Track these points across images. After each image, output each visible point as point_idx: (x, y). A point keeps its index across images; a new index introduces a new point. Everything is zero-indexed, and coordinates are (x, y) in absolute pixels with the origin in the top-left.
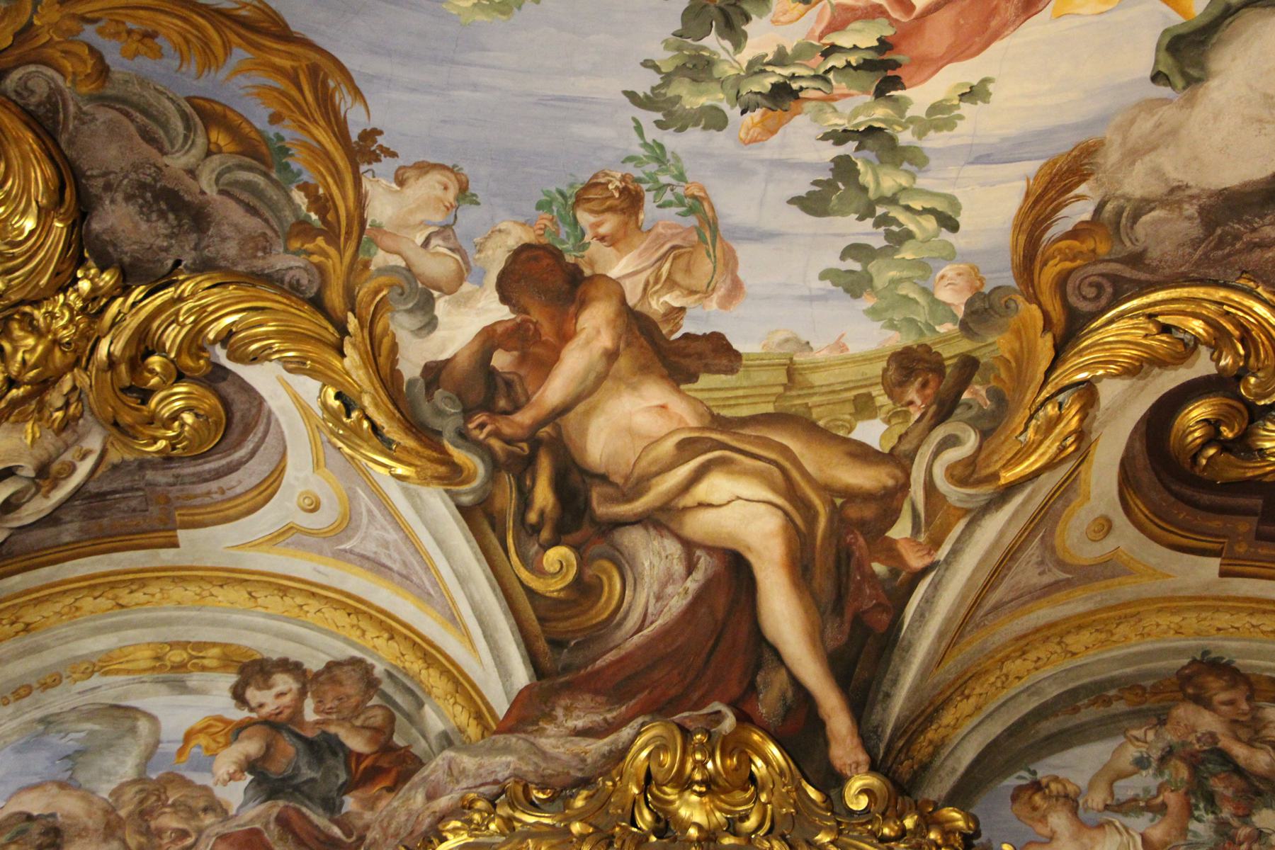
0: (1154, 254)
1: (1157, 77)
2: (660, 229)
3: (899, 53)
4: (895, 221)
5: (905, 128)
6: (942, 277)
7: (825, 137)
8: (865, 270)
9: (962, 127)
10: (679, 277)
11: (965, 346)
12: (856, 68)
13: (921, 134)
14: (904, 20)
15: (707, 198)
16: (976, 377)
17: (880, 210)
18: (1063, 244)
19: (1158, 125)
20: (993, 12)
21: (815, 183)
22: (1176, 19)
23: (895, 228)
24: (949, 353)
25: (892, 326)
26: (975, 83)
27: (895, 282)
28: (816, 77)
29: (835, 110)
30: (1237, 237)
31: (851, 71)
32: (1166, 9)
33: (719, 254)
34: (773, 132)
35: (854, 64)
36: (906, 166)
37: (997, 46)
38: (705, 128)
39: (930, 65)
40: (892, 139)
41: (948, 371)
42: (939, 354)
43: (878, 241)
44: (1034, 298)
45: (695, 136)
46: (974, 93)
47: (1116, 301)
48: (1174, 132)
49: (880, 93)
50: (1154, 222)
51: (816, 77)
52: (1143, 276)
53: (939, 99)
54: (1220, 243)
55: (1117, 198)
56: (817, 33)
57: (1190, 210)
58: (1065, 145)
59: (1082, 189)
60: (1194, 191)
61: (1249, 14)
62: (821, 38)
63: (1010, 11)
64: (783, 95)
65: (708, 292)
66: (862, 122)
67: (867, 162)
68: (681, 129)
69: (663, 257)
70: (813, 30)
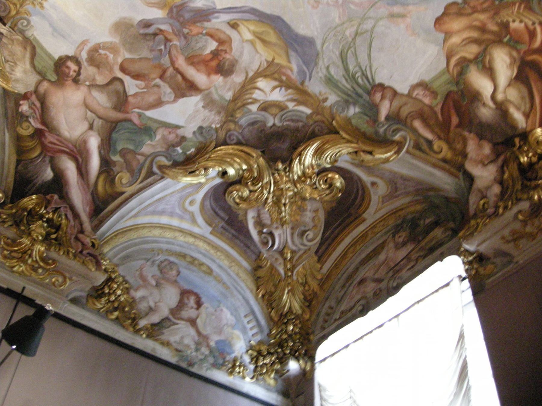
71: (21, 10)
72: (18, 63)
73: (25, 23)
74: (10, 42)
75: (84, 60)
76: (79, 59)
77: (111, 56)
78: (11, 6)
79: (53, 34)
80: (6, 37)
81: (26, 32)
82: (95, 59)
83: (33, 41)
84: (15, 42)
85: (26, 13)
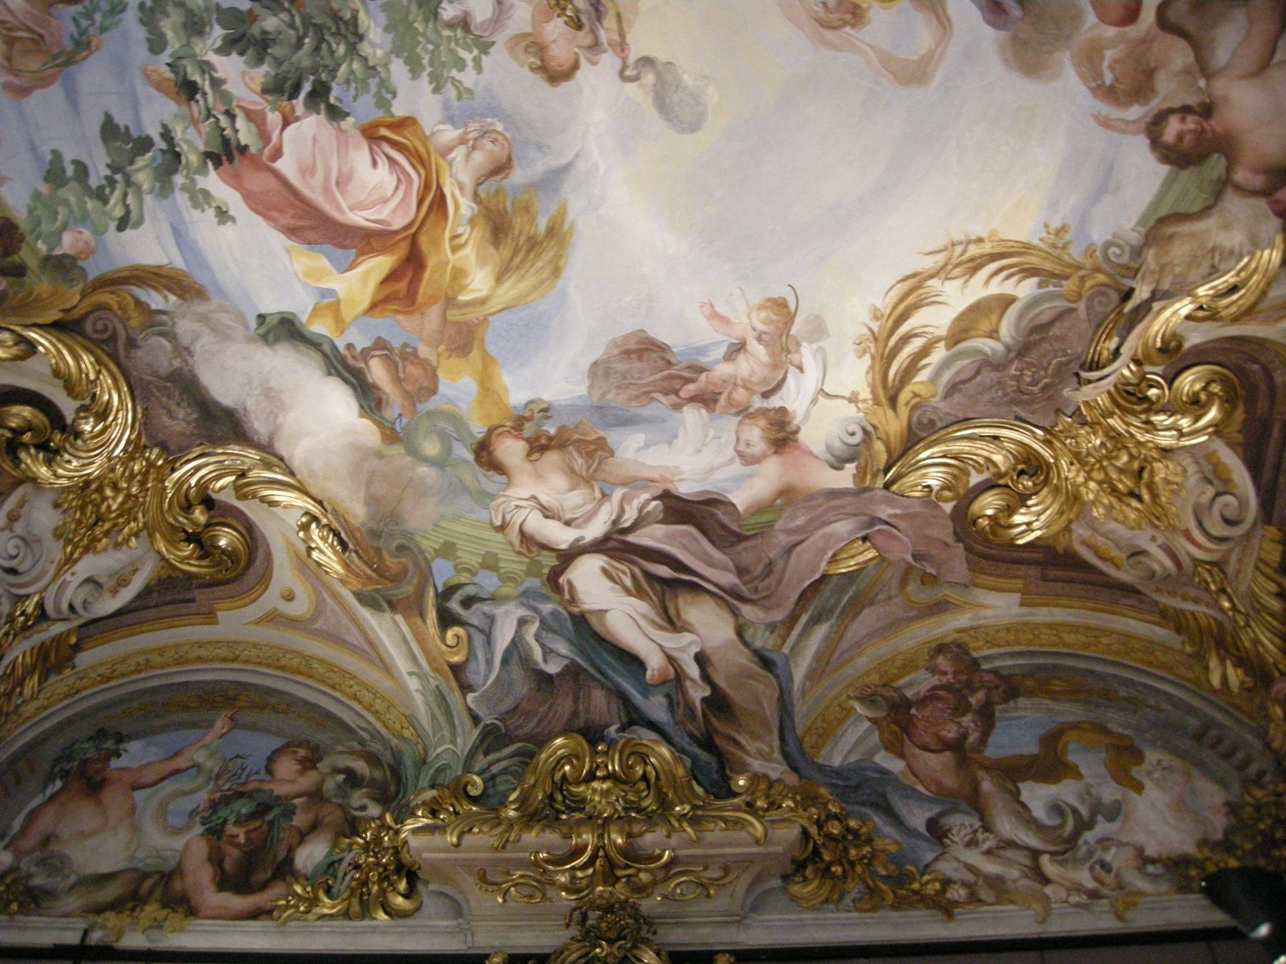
0: (139, 353)
1: (262, 318)
2: (54, 23)
4: (113, 189)
5: (186, 177)
6: (80, 232)
7: (165, 126)
8: (69, 180)
9: (196, 214)
10: (18, 46)
11: (32, 263)
13: (184, 189)
14: (264, 158)
15: (91, 53)
16: (11, 279)
17: (118, 177)
18: (129, 298)
19: (229, 327)
20: (281, 211)
21: (127, 128)
22: (304, 319)
23: (107, 191)
24: (24, 255)
25: (31, 211)
26: (231, 213)
27: (66, 203)
28: (208, 110)
29: (186, 128)
30: (169, 397)
33: (49, 72)
34: (158, 89)
36: (158, 185)
38: (148, 40)
39: (236, 182)
40: (175, 171)
41: (10, 259)
42: (20, 249)
43: (94, 182)
44: (84, 295)
45: (140, 33)
46: (223, 215)
47: (98, 343)
48: (227, 337)
49: (208, 155)
50: (161, 346)
51: (208, 110)
52: (121, 352)
53: (215, 193)
54: (158, 388)
55: (172, 319)
57: (177, 363)
58: (201, 278)
59: (173, 298)
60: (190, 361)
61: (318, 358)
62: (240, 107)
63: (287, 220)
64: (189, 90)
65: (13, 71)
66: (183, 147)
67: (153, 159)
68: (142, 22)
69: (33, 31)
71: (1088, 263)
72: (1210, 245)
73: (1113, 250)
74: (1168, 270)
75: (1146, 109)
76: (1148, 120)
77: (1109, 54)
78: (1088, 284)
79: (1116, 190)
80: (1158, 282)
81: (1134, 242)
82: (1135, 83)
83: (1148, 227)
84: (1163, 261)
85: (1091, 255)
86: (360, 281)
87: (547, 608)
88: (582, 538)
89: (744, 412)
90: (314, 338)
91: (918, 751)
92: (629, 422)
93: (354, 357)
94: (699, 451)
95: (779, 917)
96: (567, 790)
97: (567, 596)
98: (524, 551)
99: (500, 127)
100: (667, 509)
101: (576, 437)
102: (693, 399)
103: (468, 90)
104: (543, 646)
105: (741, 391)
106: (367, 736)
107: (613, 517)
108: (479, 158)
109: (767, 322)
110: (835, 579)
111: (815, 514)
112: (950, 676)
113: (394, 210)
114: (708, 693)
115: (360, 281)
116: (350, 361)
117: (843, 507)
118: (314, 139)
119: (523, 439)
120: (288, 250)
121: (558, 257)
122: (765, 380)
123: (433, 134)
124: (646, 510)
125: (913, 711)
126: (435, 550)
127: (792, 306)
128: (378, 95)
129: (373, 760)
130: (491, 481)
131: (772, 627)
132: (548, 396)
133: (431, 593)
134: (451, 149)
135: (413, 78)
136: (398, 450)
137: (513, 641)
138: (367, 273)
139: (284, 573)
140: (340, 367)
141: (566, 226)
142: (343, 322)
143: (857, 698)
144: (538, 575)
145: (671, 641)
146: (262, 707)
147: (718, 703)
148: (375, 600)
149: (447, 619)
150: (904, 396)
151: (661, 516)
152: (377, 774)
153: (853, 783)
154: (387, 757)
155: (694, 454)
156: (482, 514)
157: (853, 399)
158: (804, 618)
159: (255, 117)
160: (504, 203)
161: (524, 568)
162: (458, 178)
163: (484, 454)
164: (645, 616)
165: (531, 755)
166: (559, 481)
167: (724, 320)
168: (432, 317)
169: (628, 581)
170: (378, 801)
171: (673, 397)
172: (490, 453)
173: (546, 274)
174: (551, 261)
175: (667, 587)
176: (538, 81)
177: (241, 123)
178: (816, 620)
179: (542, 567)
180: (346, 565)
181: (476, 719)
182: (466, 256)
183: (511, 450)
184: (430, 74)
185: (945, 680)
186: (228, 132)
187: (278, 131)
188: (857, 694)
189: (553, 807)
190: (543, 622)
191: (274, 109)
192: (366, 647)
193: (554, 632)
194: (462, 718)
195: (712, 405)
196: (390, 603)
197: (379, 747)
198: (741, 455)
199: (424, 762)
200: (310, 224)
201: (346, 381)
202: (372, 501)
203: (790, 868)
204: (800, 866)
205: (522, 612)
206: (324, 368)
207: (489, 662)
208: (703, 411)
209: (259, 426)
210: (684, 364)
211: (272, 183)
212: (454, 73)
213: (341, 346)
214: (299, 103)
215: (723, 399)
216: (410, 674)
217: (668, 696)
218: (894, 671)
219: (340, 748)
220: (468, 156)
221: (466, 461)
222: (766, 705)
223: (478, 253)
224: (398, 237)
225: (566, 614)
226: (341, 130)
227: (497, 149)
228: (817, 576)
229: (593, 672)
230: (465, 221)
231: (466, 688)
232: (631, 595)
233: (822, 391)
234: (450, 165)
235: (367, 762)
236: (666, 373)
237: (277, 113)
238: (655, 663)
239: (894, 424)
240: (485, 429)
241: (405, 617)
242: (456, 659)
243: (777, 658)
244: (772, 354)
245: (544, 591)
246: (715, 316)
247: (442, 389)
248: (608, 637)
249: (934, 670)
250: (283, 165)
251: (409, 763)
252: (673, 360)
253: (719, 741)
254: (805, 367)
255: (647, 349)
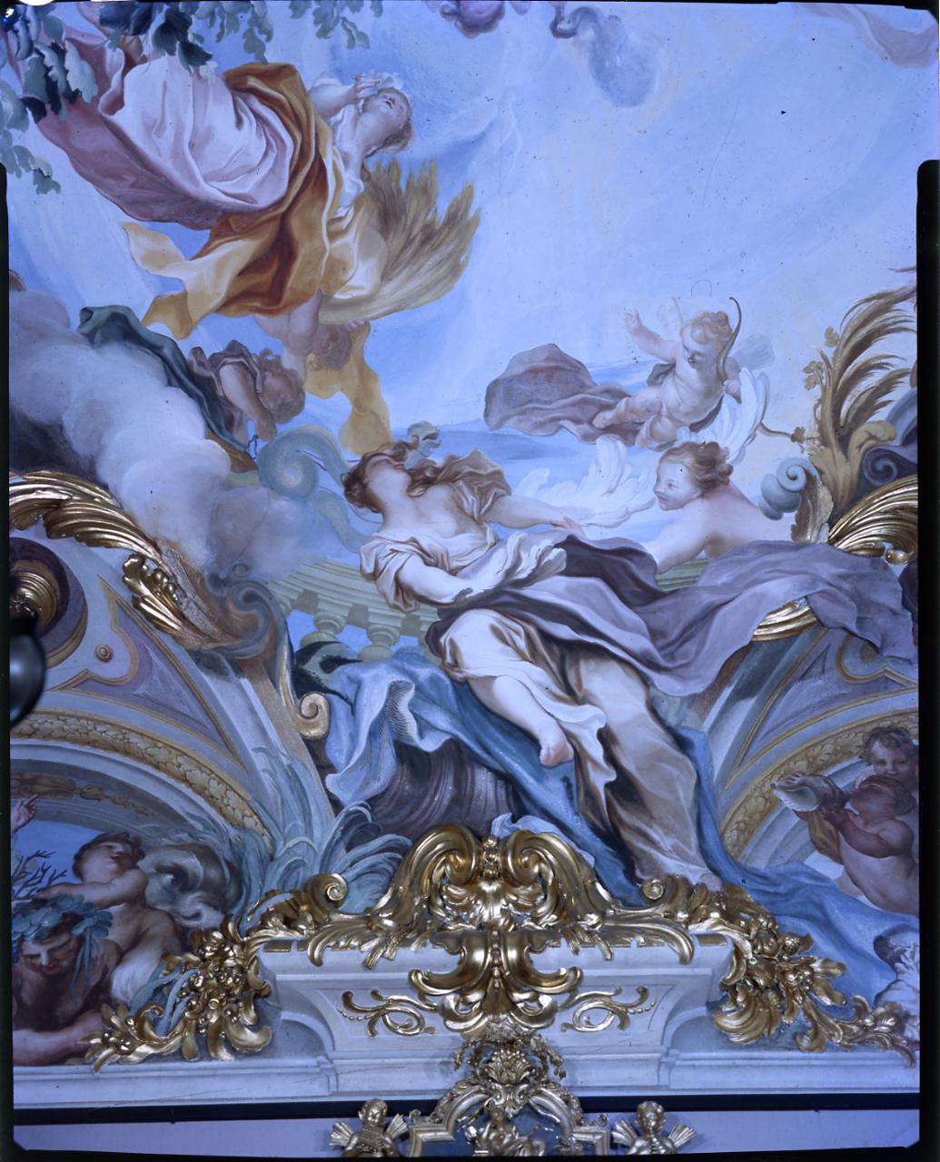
1: (87, 313)
3: (69, 110)
12: (46, 76)
14: (100, 108)
20: (118, 178)
22: (140, 314)
26: (54, 178)
28: (31, 43)
31: (43, 73)
32: (148, 304)
35: (50, 74)
37: (90, 186)
39: (62, 138)
46: (44, 181)
49: (29, 103)
51: (31, 43)
53: (34, 153)
56: (73, 36)
61: (157, 364)
62: (71, 40)
63: (123, 188)
70: (76, 31)
86: (212, 269)
87: (424, 673)
88: (469, 590)
89: (669, 449)
90: (154, 340)
91: (855, 853)
92: (532, 453)
93: (201, 364)
94: (611, 491)
95: (707, 1055)
96: (448, 893)
97: (449, 659)
98: (400, 604)
99: (398, 87)
100: (570, 558)
101: (467, 469)
102: (609, 429)
103: (363, 36)
104: (416, 717)
105: (667, 421)
106: (199, 826)
107: (507, 567)
108: (371, 122)
109: (704, 340)
110: (765, 646)
111: (743, 571)
112: (889, 767)
113: (261, 184)
114: (613, 778)
115: (212, 269)
116: (196, 368)
117: (778, 563)
118: (165, 86)
119: (404, 470)
120: (124, 228)
121: (460, 251)
122: (695, 410)
123: (314, 89)
124: (546, 560)
125: (848, 806)
126: (292, 601)
127: (733, 323)
128: (249, 35)
129: (207, 855)
130: (362, 520)
131: (693, 700)
132: (437, 418)
133: (286, 654)
134: (336, 110)
135: (294, 16)
136: (252, 477)
137: (383, 712)
138: (225, 259)
139: (101, 625)
140: (183, 377)
141: (471, 214)
142: (190, 320)
143: (783, 788)
144: (417, 634)
145: (572, 715)
146: (66, 791)
147: (625, 788)
148: (214, 659)
149: (304, 685)
150: (858, 437)
151: (564, 567)
152: (214, 873)
153: (781, 889)
154: (225, 852)
155: (607, 492)
156: (351, 560)
157: (797, 437)
158: (727, 692)
159: (92, 56)
160: (398, 181)
161: (399, 625)
162: (344, 146)
163: (356, 486)
164: (539, 684)
165: (406, 851)
166: (446, 522)
167: (651, 336)
168: (301, 318)
169: (522, 643)
170: (216, 908)
171: (585, 427)
172: (364, 486)
173: (444, 269)
174: (450, 255)
175: (566, 652)
176: (450, 29)
177: (72, 60)
178: (742, 693)
179: (420, 623)
180: (180, 615)
181: (336, 805)
182: (347, 245)
183: (388, 483)
184: (316, 13)
185: (881, 769)
186: (54, 73)
187: (119, 73)
188: (783, 783)
189: (430, 913)
190: (417, 689)
191: (117, 44)
192: (202, 717)
193: (433, 701)
194: (319, 805)
195: (630, 437)
196: (232, 662)
197: (215, 840)
198: (663, 498)
199: (272, 858)
200: (154, 196)
201: (191, 394)
202: (217, 541)
203: (717, 995)
204: (730, 989)
205: (397, 677)
206: (164, 376)
207: (354, 738)
208: (620, 444)
209: (79, 443)
210: (600, 387)
211: (109, 141)
212: (347, 13)
213: (185, 348)
214: (148, 39)
215: (644, 431)
216: (257, 750)
217: (565, 780)
218: (826, 757)
219: (165, 841)
220: (356, 120)
221: (334, 495)
222: (681, 793)
223: (361, 243)
224: (265, 217)
225: (447, 682)
226: (199, 77)
227: (393, 112)
228: (746, 642)
229: (478, 750)
230: (348, 202)
231: (325, 768)
232: (525, 659)
233: (761, 424)
234: (334, 131)
235: (200, 857)
236: (579, 397)
237: (119, 50)
238: (550, 740)
239: (845, 470)
240: (359, 458)
241: (251, 680)
242: (314, 733)
243: (696, 739)
244: (705, 379)
245: (422, 653)
246: (641, 331)
247: (307, 406)
248: (496, 711)
249: (867, 757)
250: (119, 118)
251: (252, 859)
252: (587, 382)
253: (627, 836)
254: (742, 397)
255: (557, 368)
